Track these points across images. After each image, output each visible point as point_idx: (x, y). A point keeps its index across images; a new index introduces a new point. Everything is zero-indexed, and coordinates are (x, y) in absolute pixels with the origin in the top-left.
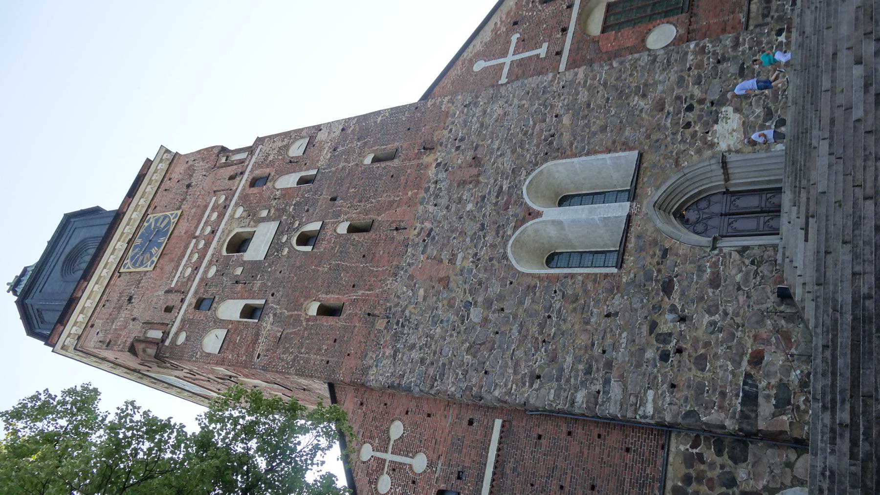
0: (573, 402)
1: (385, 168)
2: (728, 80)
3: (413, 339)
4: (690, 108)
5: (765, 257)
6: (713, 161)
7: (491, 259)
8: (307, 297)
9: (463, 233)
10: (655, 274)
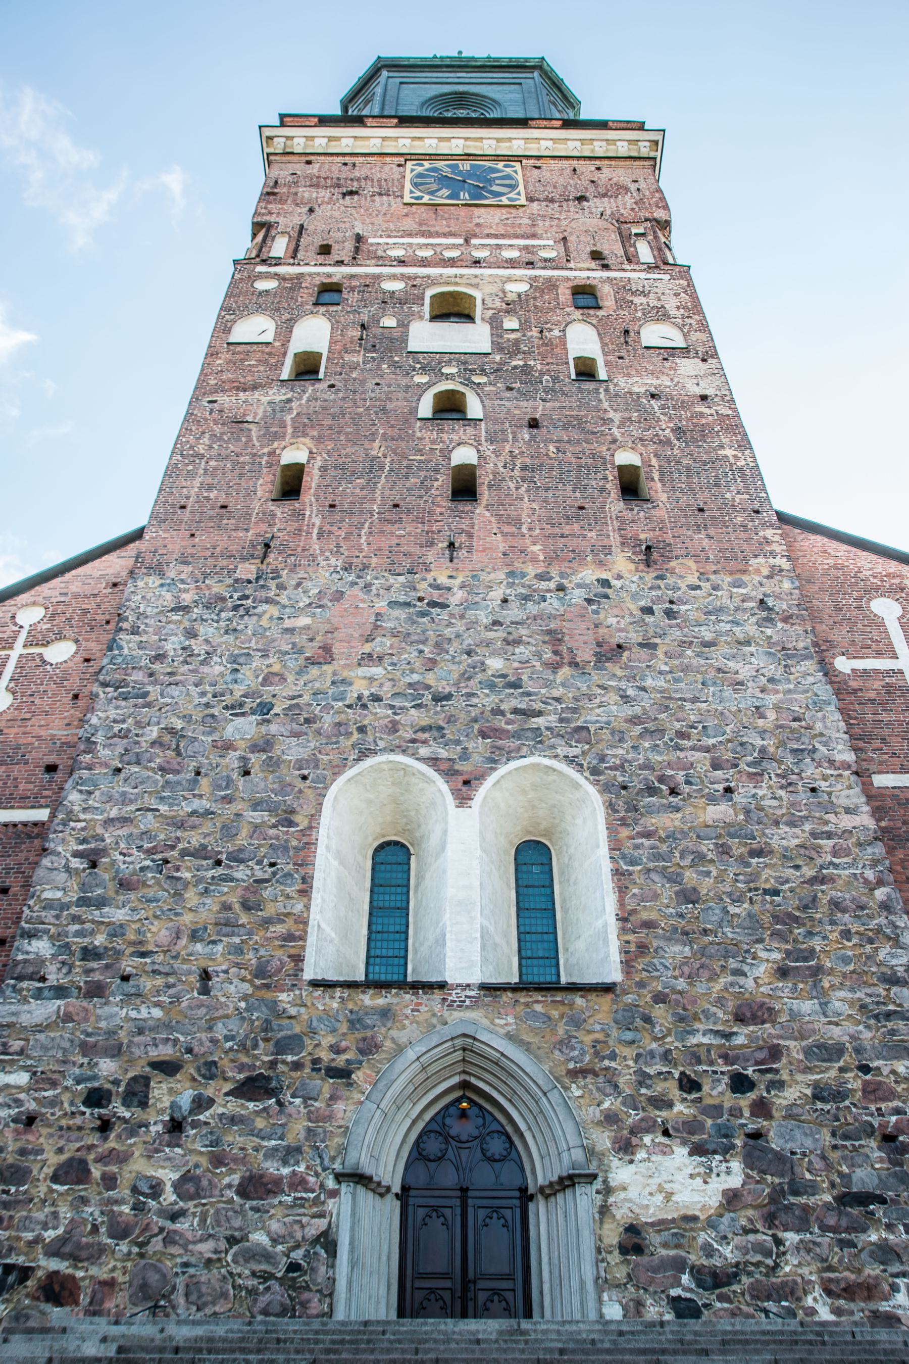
0: (31, 935)
1: (602, 490)
2: (829, 1167)
3: (206, 630)
4: (740, 1084)
5: (306, 1295)
6: (578, 1155)
7: (362, 730)
8: (319, 440)
9: (431, 665)
10: (289, 1058)
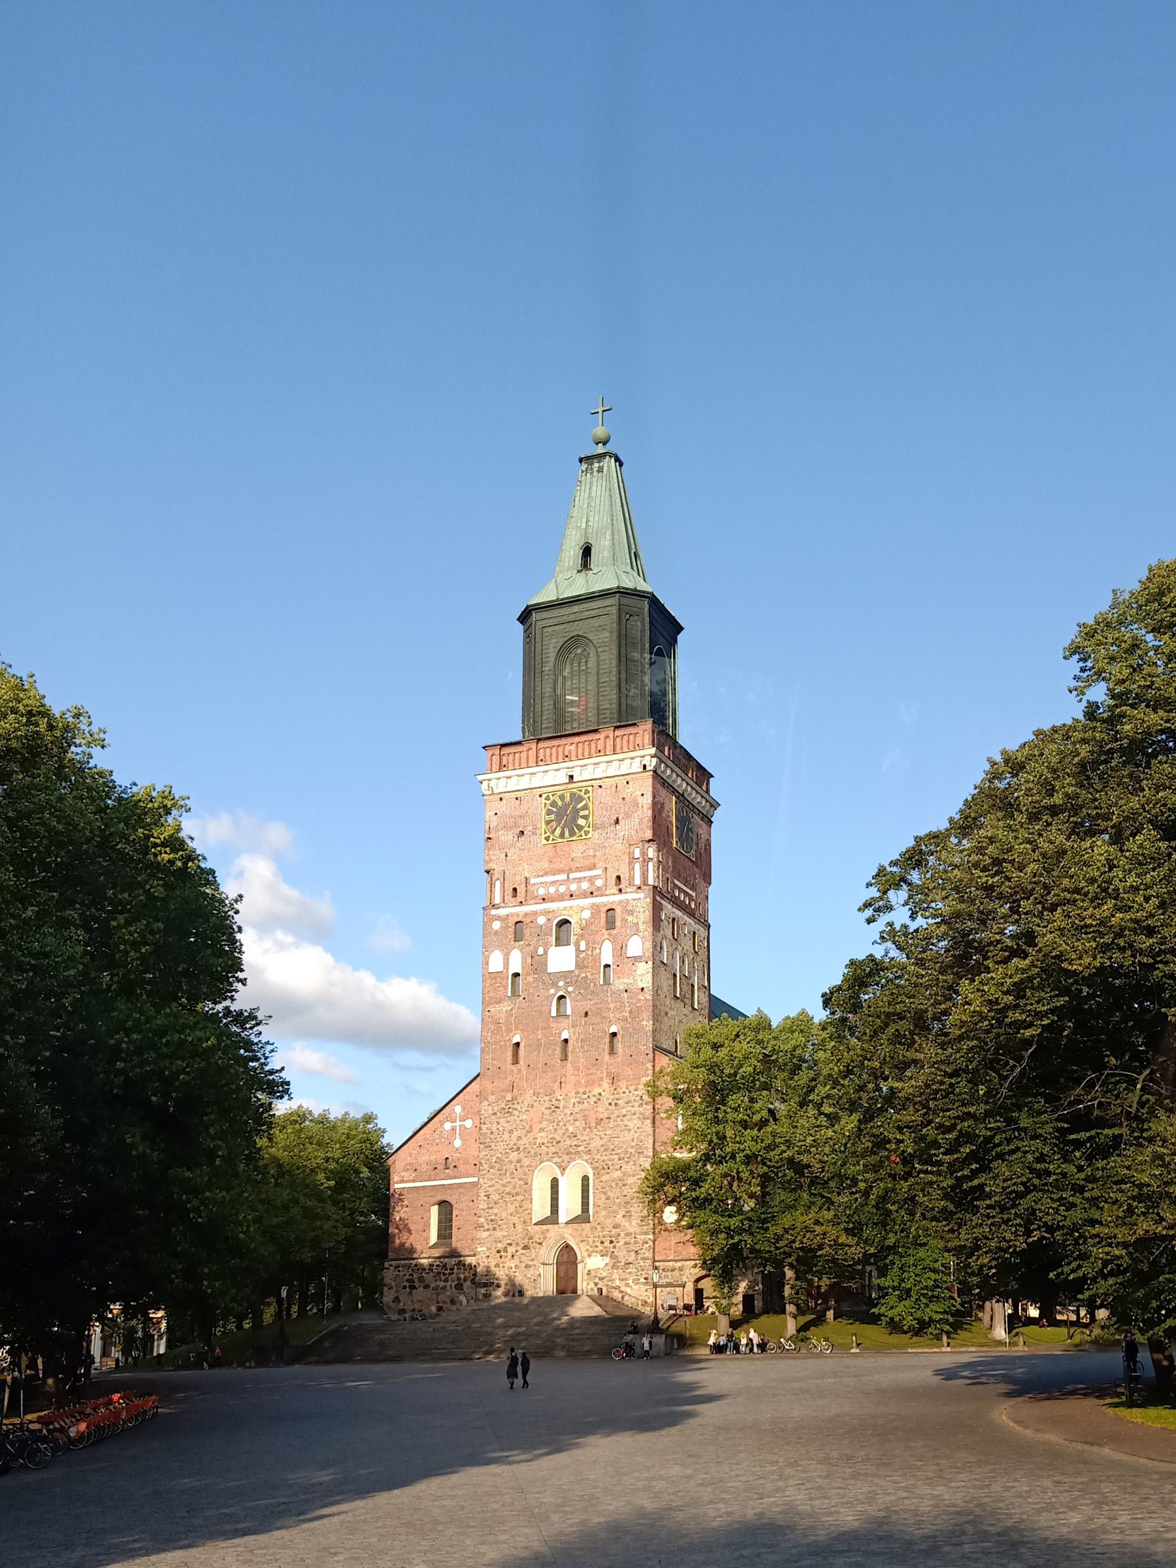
3: (502, 1121)
4: (611, 1242)
8: (522, 1031)
